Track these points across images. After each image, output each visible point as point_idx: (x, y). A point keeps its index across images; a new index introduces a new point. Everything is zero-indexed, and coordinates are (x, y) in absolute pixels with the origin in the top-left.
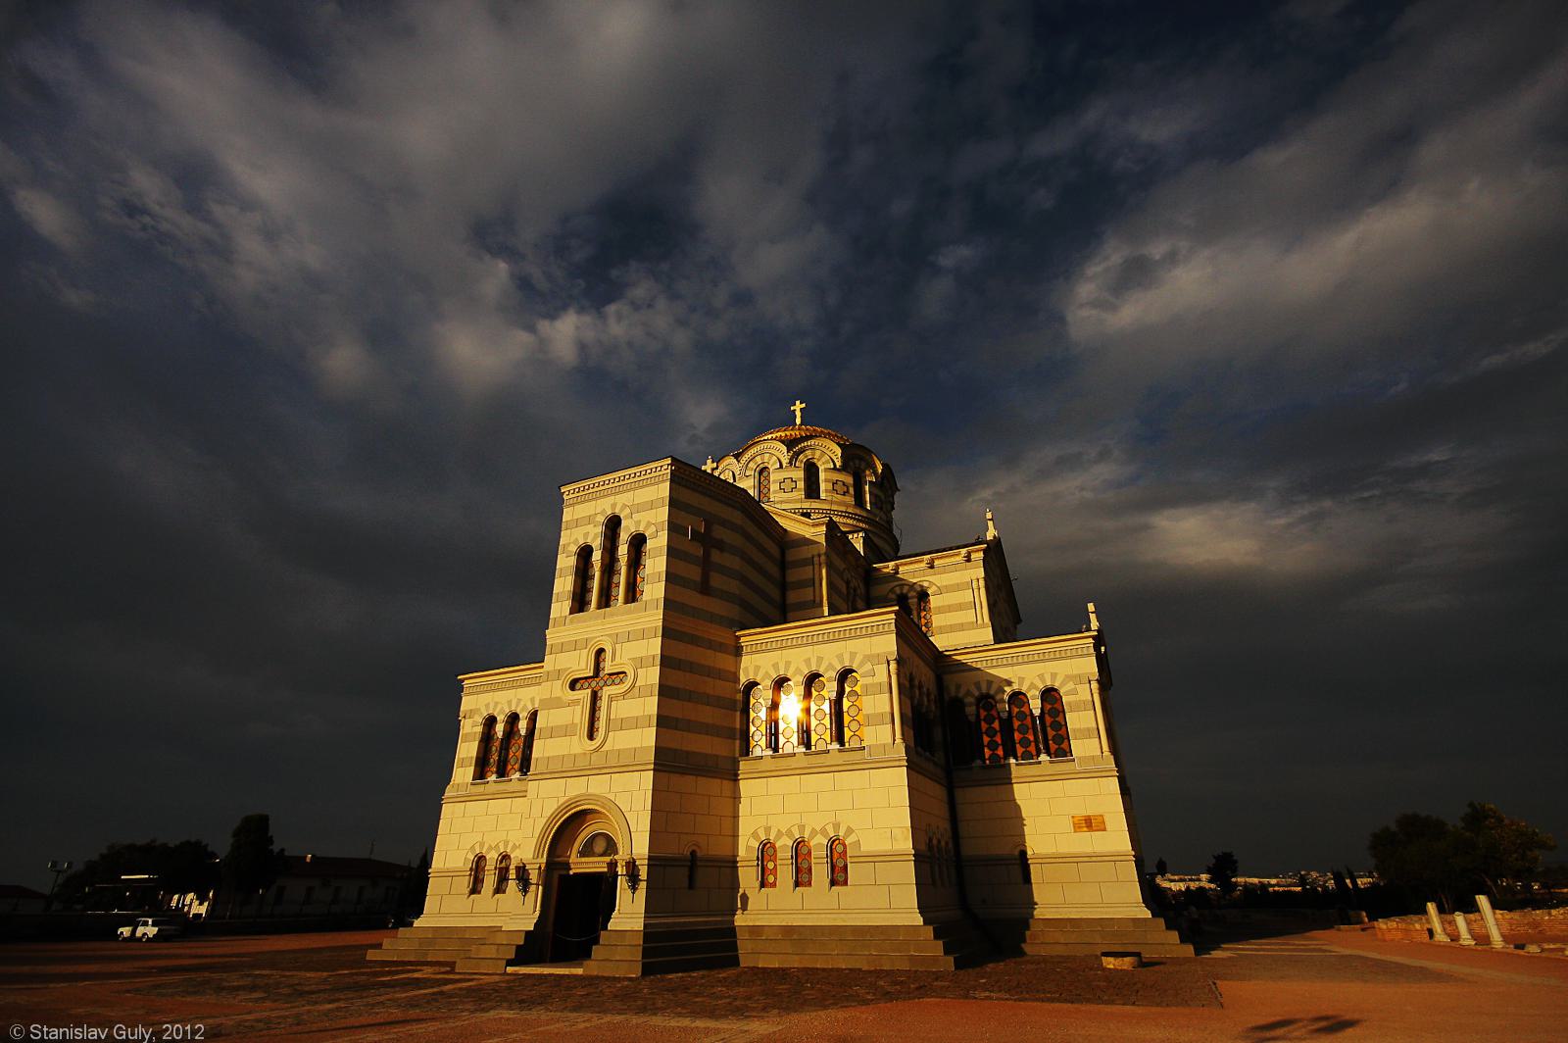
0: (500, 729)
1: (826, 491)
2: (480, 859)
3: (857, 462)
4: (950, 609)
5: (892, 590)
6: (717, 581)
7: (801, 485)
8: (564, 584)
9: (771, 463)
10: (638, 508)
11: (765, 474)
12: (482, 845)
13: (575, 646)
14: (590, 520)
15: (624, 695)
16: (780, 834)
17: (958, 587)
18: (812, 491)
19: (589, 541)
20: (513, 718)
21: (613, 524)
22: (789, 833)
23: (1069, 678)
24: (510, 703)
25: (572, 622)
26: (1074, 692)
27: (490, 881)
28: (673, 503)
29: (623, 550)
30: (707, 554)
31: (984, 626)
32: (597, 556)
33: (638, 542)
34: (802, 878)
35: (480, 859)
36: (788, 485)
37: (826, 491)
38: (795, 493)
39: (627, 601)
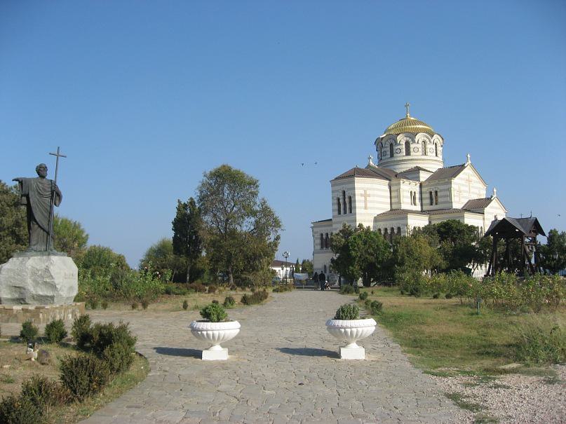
0: (324, 237)
2: (325, 266)
4: (441, 197)
6: (369, 205)
13: (340, 222)
14: (338, 191)
17: (444, 190)
21: (344, 192)
28: (354, 188)
29: (347, 200)
30: (366, 199)
32: (341, 201)
33: (350, 198)
35: (325, 266)
36: (398, 151)
38: (401, 154)
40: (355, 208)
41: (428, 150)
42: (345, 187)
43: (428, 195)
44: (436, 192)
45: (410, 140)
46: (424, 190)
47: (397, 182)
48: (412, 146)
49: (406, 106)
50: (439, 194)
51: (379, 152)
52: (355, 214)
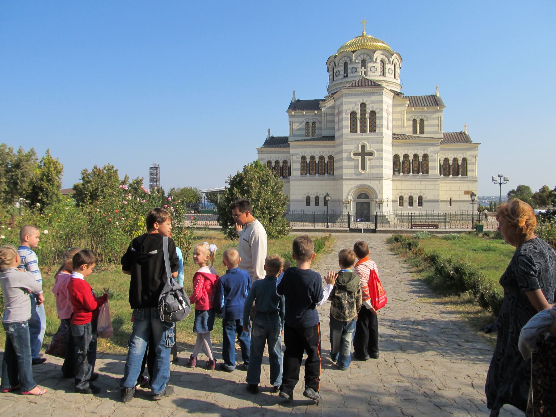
0: (308, 160)
4: (430, 126)
5: (411, 117)
7: (378, 70)
8: (347, 123)
9: (367, 59)
10: (372, 102)
12: (308, 193)
15: (372, 159)
16: (405, 194)
19: (355, 110)
20: (313, 158)
21: (363, 105)
22: (407, 194)
23: (470, 155)
24: (311, 152)
25: (352, 135)
26: (470, 160)
27: (313, 203)
29: (368, 115)
31: (441, 133)
32: (358, 116)
33: (373, 113)
34: (411, 204)
36: (373, 69)
39: (370, 131)
40: (382, 126)
41: (397, 75)
42: (366, 100)
43: (411, 123)
44: (422, 121)
45: (386, 59)
47: (401, 103)
48: (388, 66)
50: (426, 123)
52: (382, 134)
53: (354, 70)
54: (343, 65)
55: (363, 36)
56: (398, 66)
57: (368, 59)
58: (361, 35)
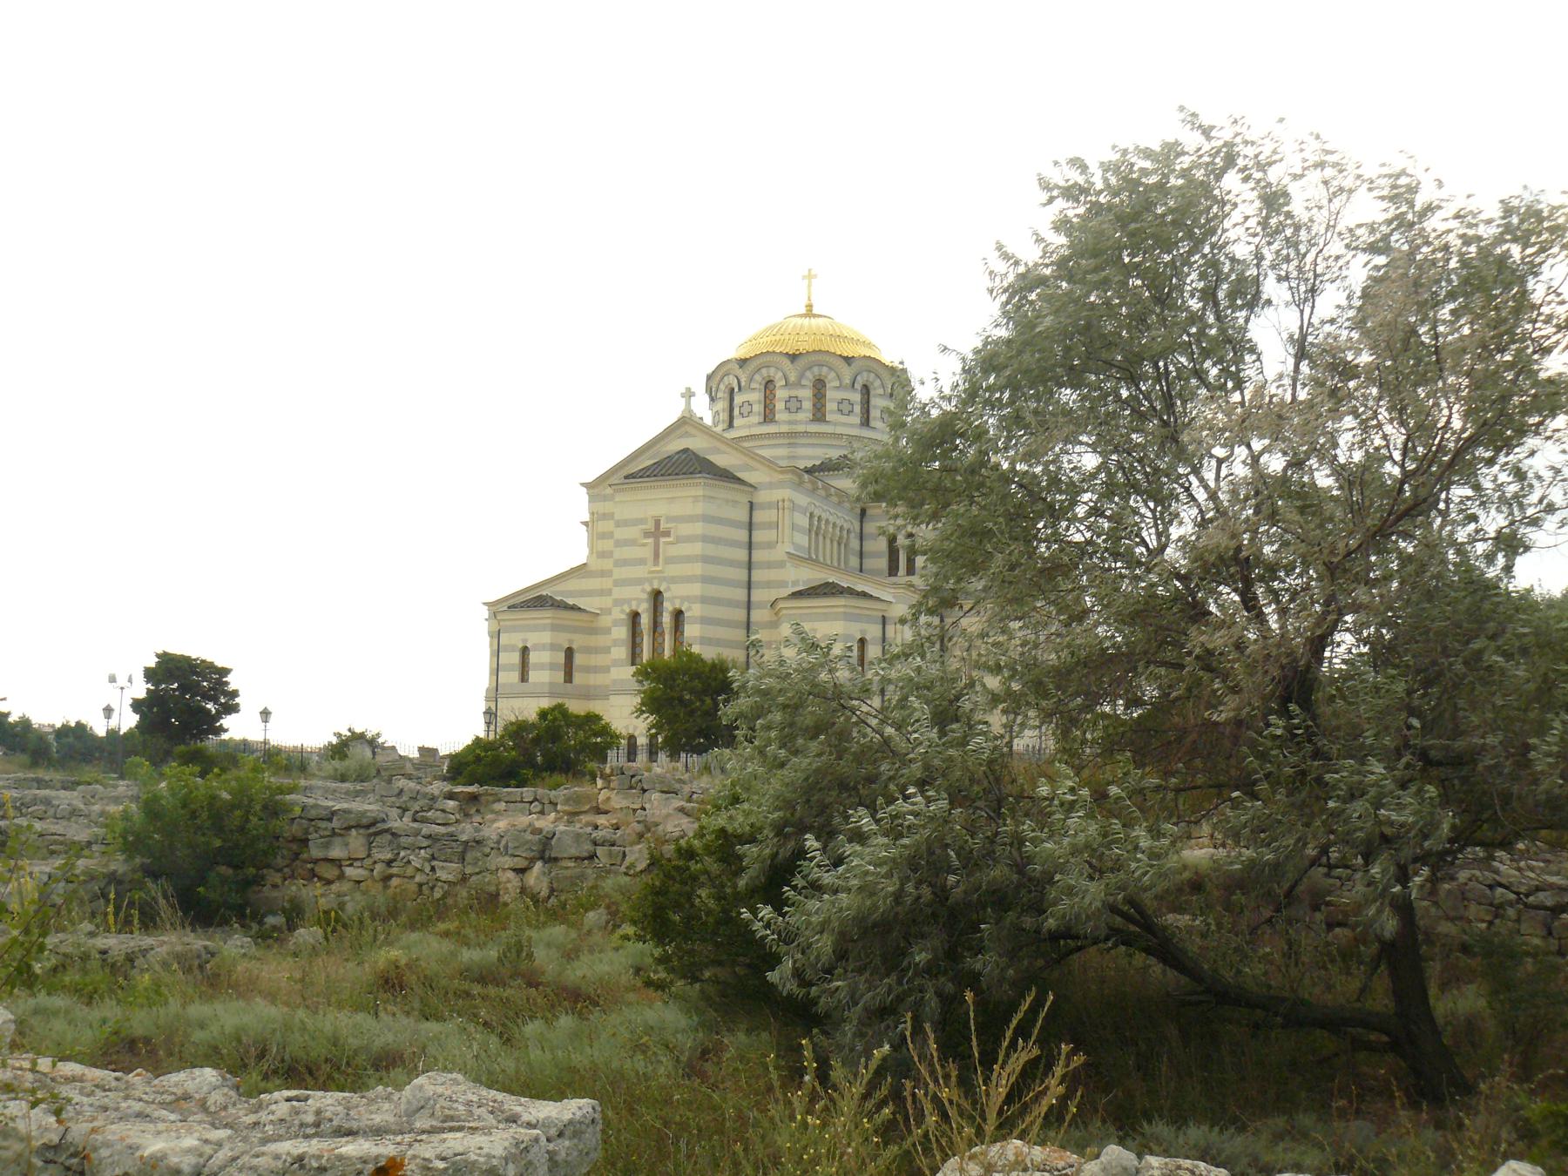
1: (832, 412)
3: (865, 374)
7: (808, 405)
11: (771, 387)
18: (819, 415)
36: (793, 405)
37: (832, 412)
38: (801, 416)
41: (875, 413)
43: (882, 544)
46: (871, 527)
48: (832, 395)
49: (810, 276)
51: (722, 405)
53: (746, 409)
54: (727, 396)
55: (809, 313)
56: (881, 391)
57: (780, 379)
58: (803, 311)
